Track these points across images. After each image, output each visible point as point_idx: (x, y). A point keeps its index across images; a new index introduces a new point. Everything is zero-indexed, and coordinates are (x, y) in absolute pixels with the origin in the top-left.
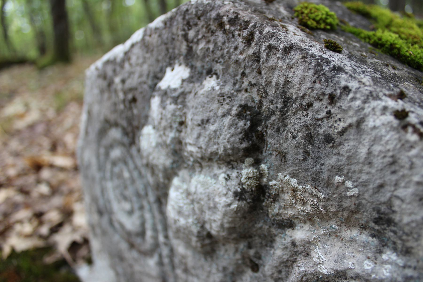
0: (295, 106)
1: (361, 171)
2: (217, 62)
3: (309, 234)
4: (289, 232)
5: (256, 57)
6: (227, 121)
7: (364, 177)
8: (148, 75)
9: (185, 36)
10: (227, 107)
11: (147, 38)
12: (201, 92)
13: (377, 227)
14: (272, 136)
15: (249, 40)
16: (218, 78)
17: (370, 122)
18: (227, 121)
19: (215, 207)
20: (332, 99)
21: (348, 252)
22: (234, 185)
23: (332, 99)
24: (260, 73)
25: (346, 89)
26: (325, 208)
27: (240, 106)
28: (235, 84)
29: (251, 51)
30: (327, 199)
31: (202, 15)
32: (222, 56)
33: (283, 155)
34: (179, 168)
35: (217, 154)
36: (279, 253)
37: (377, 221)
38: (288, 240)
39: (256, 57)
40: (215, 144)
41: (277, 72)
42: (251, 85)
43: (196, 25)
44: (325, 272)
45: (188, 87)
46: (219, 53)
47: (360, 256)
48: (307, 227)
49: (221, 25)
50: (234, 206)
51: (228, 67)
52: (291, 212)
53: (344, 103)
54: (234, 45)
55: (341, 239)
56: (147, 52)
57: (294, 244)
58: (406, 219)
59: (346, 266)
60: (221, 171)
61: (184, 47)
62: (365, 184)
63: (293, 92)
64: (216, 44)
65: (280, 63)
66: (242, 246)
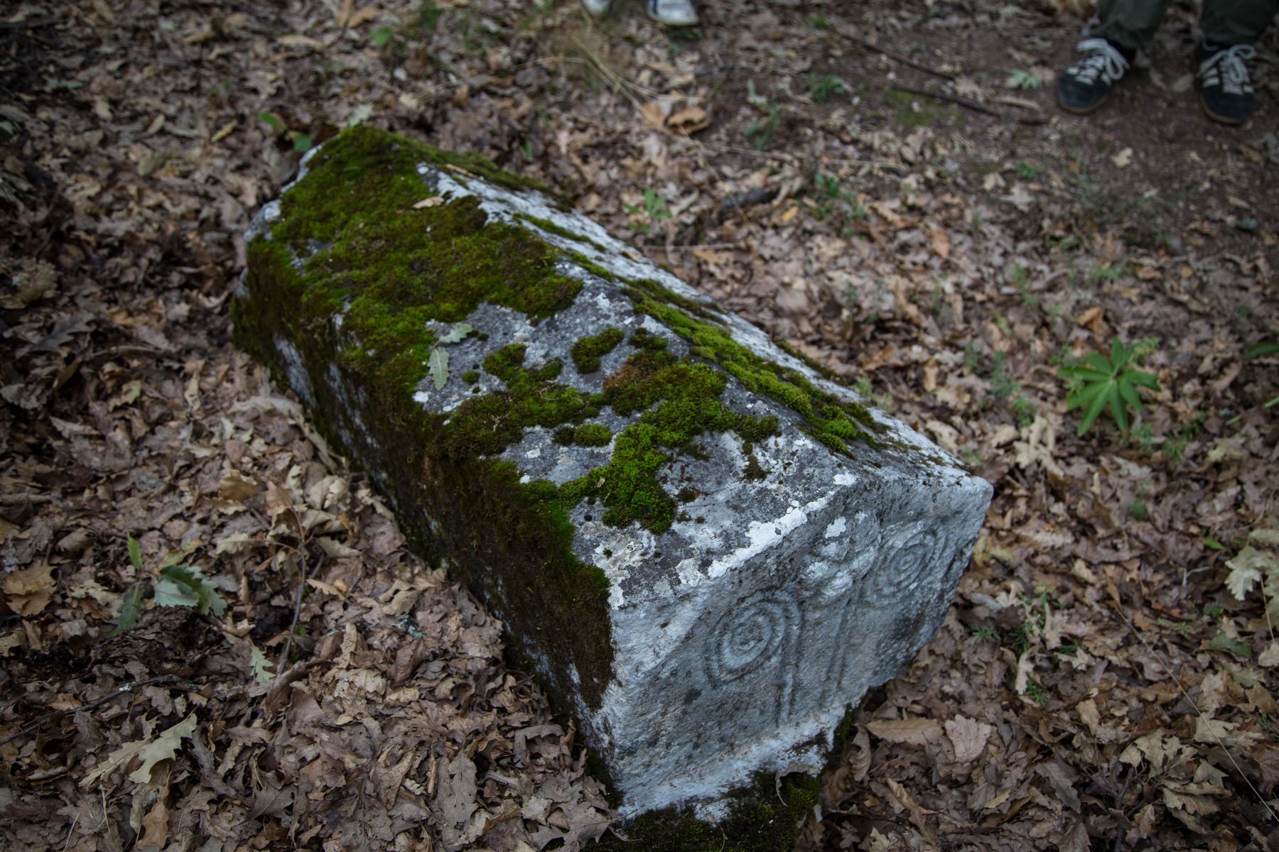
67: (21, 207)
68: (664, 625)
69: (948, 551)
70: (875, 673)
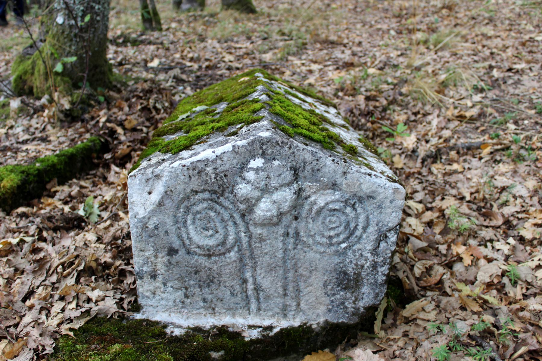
5: (294, 153)
6: (288, 172)
8: (237, 164)
9: (261, 148)
11: (237, 149)
15: (290, 148)
17: (328, 163)
18: (288, 172)
19: (286, 200)
20: (317, 160)
22: (293, 191)
23: (317, 160)
29: (291, 151)
33: (305, 177)
39: (294, 153)
49: (278, 144)
52: (309, 193)
53: (321, 160)
61: (261, 152)
63: (307, 160)
66: (293, 212)
67: (162, 111)
68: (150, 193)
69: (370, 229)
70: (330, 310)
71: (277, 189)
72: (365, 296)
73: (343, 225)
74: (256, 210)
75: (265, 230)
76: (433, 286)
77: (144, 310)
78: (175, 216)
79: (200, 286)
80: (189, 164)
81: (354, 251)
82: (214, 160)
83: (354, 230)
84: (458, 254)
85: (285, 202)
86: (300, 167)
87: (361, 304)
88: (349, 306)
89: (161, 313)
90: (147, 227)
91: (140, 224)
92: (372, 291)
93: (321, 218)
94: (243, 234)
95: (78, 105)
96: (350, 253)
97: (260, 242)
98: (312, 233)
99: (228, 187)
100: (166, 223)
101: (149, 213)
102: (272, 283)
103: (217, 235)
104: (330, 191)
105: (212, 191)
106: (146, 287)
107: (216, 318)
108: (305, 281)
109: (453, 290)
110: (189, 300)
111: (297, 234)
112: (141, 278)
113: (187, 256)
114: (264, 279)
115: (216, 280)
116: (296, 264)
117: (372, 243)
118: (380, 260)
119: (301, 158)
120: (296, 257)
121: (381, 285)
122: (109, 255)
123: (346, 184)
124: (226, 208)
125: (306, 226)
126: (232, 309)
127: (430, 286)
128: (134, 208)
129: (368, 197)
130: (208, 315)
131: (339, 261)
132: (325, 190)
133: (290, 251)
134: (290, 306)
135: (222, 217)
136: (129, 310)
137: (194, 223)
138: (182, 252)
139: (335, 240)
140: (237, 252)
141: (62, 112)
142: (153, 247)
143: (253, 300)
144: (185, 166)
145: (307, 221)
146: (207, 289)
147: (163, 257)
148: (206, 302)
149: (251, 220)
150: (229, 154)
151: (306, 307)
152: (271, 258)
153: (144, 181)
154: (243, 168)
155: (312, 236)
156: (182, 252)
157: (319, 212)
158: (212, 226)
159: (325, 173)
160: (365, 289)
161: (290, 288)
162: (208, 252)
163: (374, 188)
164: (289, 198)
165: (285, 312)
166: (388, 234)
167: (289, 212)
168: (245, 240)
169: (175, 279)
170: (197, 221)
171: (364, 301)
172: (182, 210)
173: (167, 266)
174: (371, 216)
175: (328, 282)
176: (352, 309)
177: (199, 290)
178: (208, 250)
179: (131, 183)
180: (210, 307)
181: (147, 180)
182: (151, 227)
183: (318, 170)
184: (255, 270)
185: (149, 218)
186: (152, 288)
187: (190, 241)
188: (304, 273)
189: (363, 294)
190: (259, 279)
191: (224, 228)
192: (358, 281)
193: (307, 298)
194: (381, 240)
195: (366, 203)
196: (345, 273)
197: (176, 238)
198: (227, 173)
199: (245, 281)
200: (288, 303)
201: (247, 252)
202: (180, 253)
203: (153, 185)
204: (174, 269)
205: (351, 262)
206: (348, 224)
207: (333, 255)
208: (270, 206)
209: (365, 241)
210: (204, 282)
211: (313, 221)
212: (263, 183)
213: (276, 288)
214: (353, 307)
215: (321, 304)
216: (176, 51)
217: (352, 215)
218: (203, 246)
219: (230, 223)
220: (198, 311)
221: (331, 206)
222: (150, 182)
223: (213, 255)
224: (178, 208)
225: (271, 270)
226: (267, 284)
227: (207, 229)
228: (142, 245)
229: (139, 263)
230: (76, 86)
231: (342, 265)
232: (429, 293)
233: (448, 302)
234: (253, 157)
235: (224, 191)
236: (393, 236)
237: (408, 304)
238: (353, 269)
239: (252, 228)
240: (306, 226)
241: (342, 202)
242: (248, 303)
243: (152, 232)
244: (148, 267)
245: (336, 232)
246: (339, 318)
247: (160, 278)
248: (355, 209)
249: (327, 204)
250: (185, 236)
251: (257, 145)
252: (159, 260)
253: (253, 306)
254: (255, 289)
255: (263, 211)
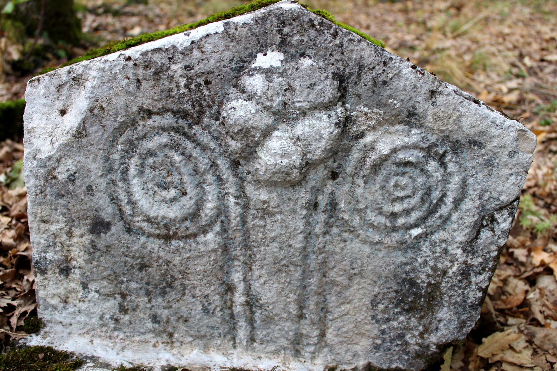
0: (366, 69)
1: (401, 95)
2: (309, 48)
3: (373, 137)
4: (361, 141)
5: (341, 45)
6: (328, 82)
7: (402, 97)
8: (231, 61)
9: (280, 32)
10: (325, 74)
12: (303, 67)
13: (408, 120)
14: (352, 87)
15: (335, 35)
16: (310, 58)
18: (328, 82)
19: (321, 138)
20: (385, 63)
21: (395, 137)
22: (334, 119)
23: (385, 63)
24: (343, 54)
25: (391, 59)
26: (383, 118)
27: (332, 73)
28: (324, 61)
29: (337, 41)
30: (385, 113)
31: (297, 18)
32: (314, 45)
33: (359, 96)
34: (278, 124)
35: (322, 103)
36: (355, 156)
37: (408, 117)
38: (362, 145)
39: (341, 45)
40: (321, 97)
41: (355, 53)
42: (337, 61)
43: (291, 24)
44: (386, 153)
45: (287, 66)
46: (311, 43)
47: (401, 137)
48: (371, 133)
49: (313, 26)
50: (335, 133)
51: (320, 50)
52: (363, 128)
53: (391, 65)
54: (324, 38)
55: (390, 133)
56: (232, 42)
57: (365, 146)
58: (421, 111)
59: (397, 144)
60: (322, 114)
61: (278, 39)
62: (402, 100)
63: (366, 62)
64: (309, 36)
65: (356, 48)
66: (330, 163)
68: (63, 113)
69: (467, 205)
70: (377, 347)
71: (304, 114)
72: (441, 325)
73: (420, 194)
74: (260, 154)
75: (274, 194)
76: (515, 309)
77: (47, 329)
78: (107, 159)
79: (148, 293)
80: (138, 56)
81: (433, 244)
82: (186, 49)
83: (437, 204)
84: (543, 264)
85: (318, 140)
86: (351, 74)
87: (433, 339)
88: (412, 341)
89: (76, 337)
90: (54, 178)
91: (42, 171)
92: (455, 318)
93: (380, 178)
94: (232, 200)
95: (30, 56)
96: (425, 247)
97: (263, 217)
98: (362, 206)
99: (210, 107)
100: (89, 171)
101: (59, 150)
102: (279, 294)
103: (184, 200)
104: (402, 127)
105: (178, 111)
106: (52, 289)
107: (175, 351)
108: (339, 294)
109: (546, 317)
110: (127, 317)
111: (333, 205)
112: (43, 272)
113: (127, 236)
114: (266, 287)
115: (177, 284)
116: (325, 262)
117: (467, 231)
118: (477, 261)
119: (354, 56)
120: (327, 248)
121: (473, 307)
122: (12, 233)
123: (435, 114)
124: (204, 148)
125: (351, 192)
126: (205, 336)
127: (510, 309)
128: (33, 140)
129: (470, 142)
130: (161, 346)
131: (404, 260)
132: (392, 124)
133: (317, 236)
134: (308, 336)
135: (196, 166)
136: (19, 329)
137: (141, 173)
138: (117, 228)
139: (401, 221)
140: (218, 233)
141: (8, 62)
142: (64, 215)
143: (242, 323)
144: (129, 59)
145: (353, 183)
146: (160, 300)
147: (82, 236)
148: (159, 322)
149: (249, 173)
150: (215, 40)
151: (337, 340)
152: (281, 248)
153: (53, 88)
154: (241, 68)
155: (359, 211)
156: (117, 228)
157: (377, 167)
158: (176, 181)
159: (397, 89)
160: (444, 313)
161: (311, 304)
162: (164, 231)
163: (483, 127)
164: (326, 132)
165: (298, 347)
166: (497, 216)
167: (322, 161)
168: (235, 211)
169: (103, 278)
170: (148, 171)
171: (439, 334)
172: (120, 147)
173: (90, 253)
174: (471, 180)
175: (380, 297)
176: (417, 348)
177: (146, 299)
178: (166, 226)
179: (30, 93)
180: (165, 331)
181: (60, 87)
182: (62, 177)
183: (385, 83)
184: (251, 270)
185: (59, 161)
186: (61, 291)
187: (133, 209)
188: (339, 279)
189: (440, 321)
190: (256, 286)
191: (197, 186)
192: (433, 299)
193: (339, 324)
194: (482, 226)
195: (464, 155)
196: (413, 283)
197: (108, 200)
198: (210, 77)
199: (230, 289)
200: (304, 332)
201: (238, 235)
202: (113, 229)
203: (68, 97)
204: (102, 259)
205: (426, 262)
206: (428, 191)
207: (395, 248)
208: (288, 145)
209: (455, 226)
210: (156, 286)
211: (365, 183)
212: (279, 99)
213: (287, 304)
214: (418, 344)
215: (362, 335)
216: (161, 23)
217: (438, 175)
218: (156, 218)
219: (210, 178)
220: (143, 337)
221: (401, 156)
222: (65, 91)
223: (175, 236)
224: (113, 142)
225: (280, 270)
226: (269, 295)
227: (165, 187)
228: (44, 212)
229: (39, 244)
230: (30, 32)
231: (408, 268)
232: (511, 321)
233: (546, 336)
234: (263, 49)
235: (201, 113)
236: (505, 220)
237: (486, 336)
238: (428, 276)
239: (250, 189)
240: (351, 192)
241: (422, 149)
242: (234, 328)
243: (64, 188)
244: (56, 252)
245: (405, 206)
246: (391, 361)
247: (76, 274)
248: (443, 165)
249: (394, 151)
250: (123, 197)
251: (272, 25)
252: (75, 240)
253: (242, 334)
254: (248, 303)
255: (275, 155)
